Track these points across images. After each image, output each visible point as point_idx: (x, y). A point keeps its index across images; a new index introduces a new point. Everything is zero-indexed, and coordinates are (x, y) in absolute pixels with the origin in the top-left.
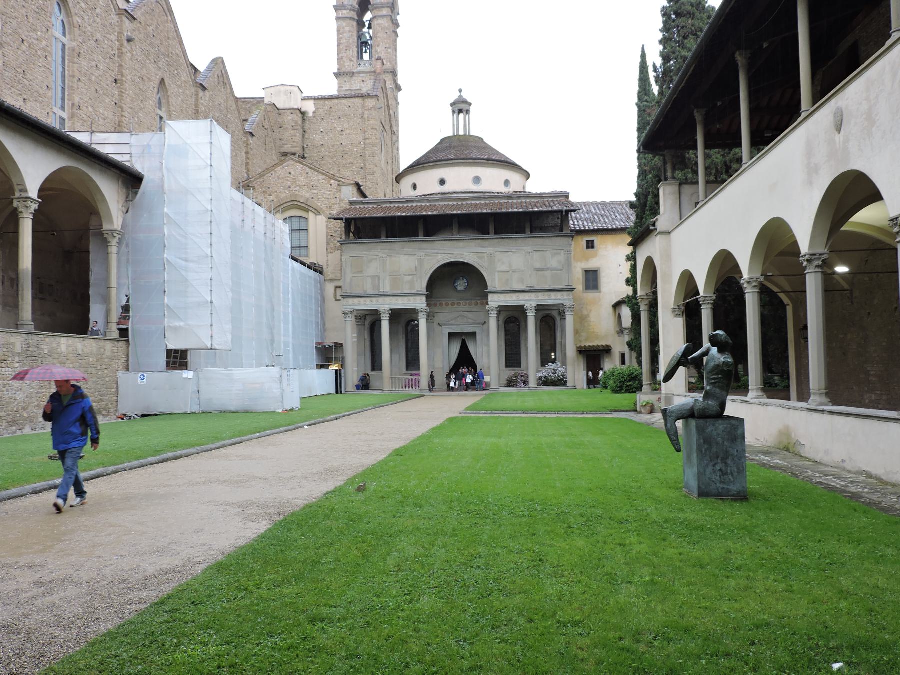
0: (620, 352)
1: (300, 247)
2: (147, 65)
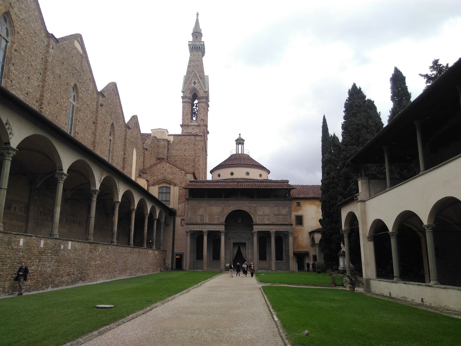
1: (166, 200)
2: (107, 116)
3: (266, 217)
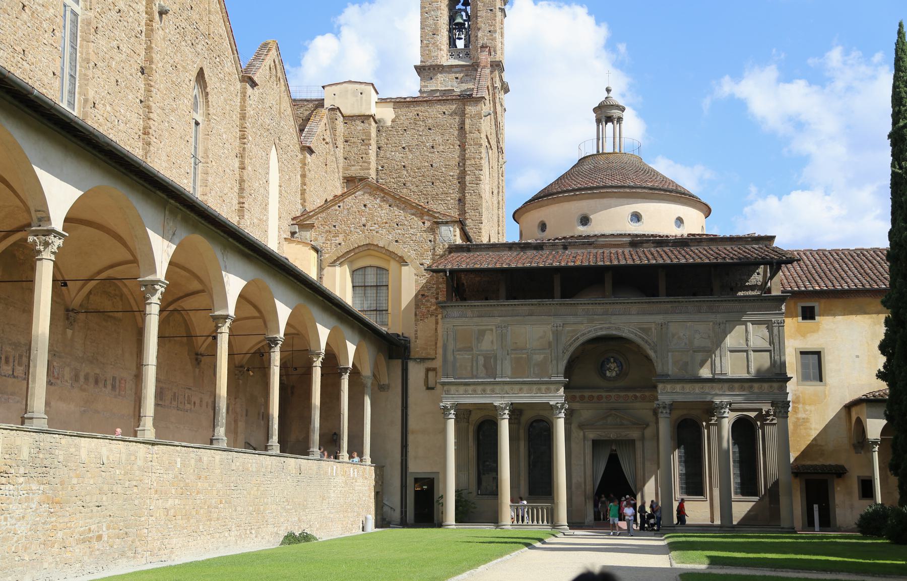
0: (858, 477)
2: (182, 48)
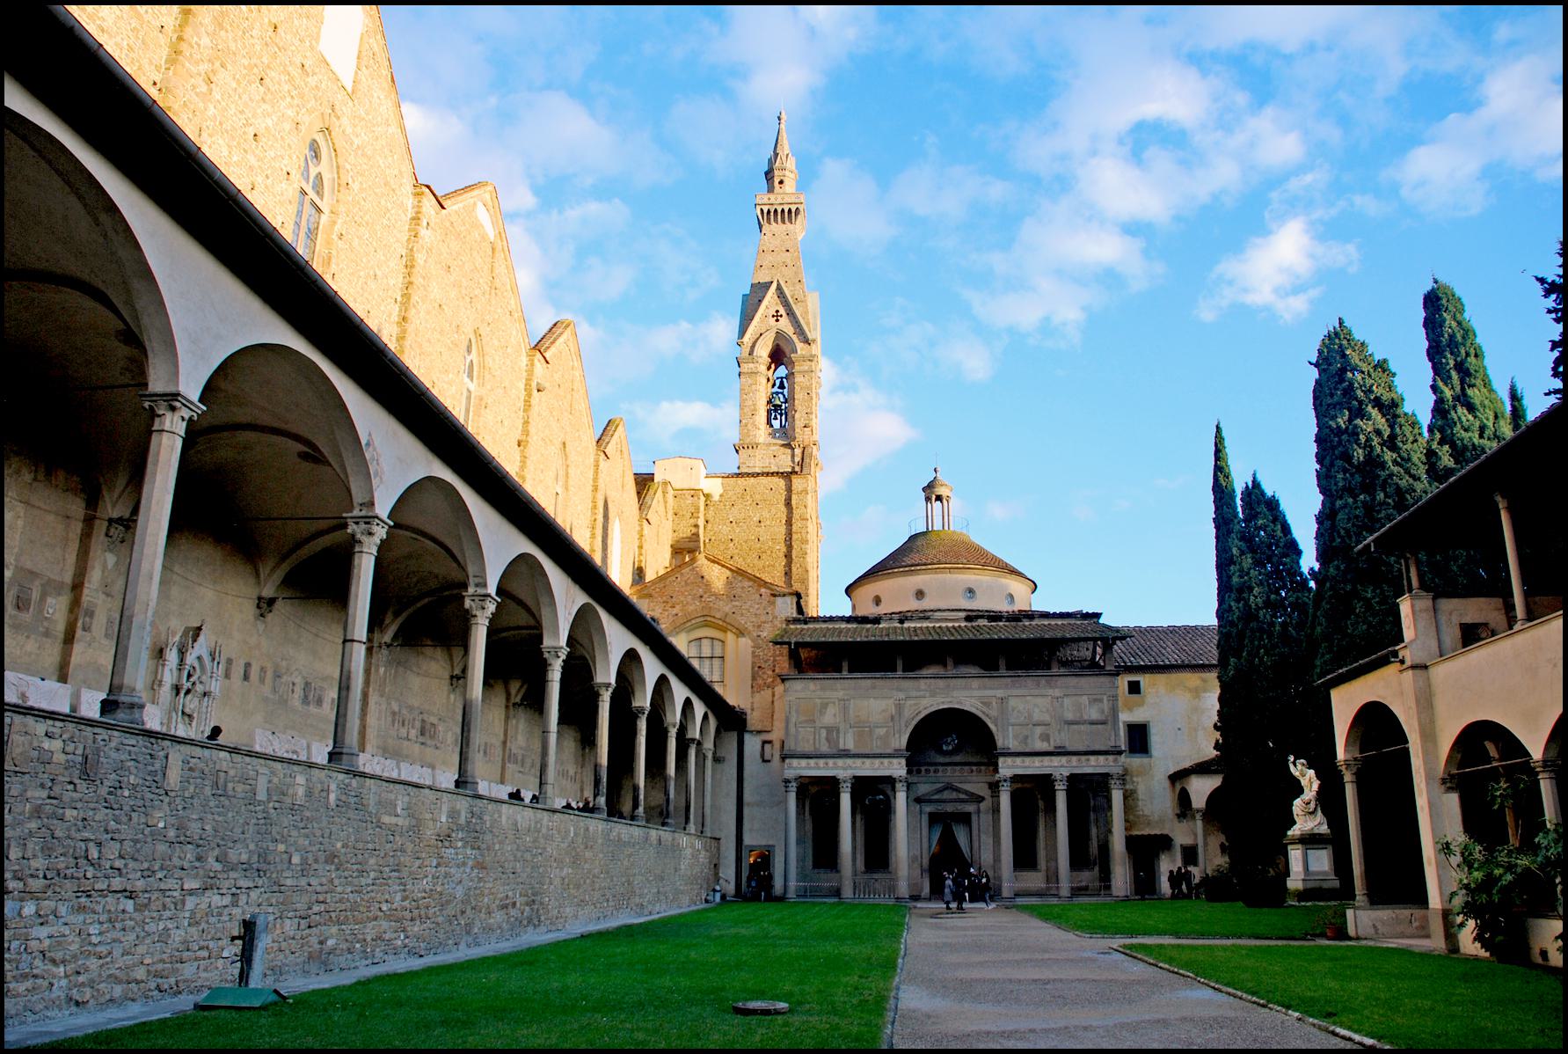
3: (1039, 730)
